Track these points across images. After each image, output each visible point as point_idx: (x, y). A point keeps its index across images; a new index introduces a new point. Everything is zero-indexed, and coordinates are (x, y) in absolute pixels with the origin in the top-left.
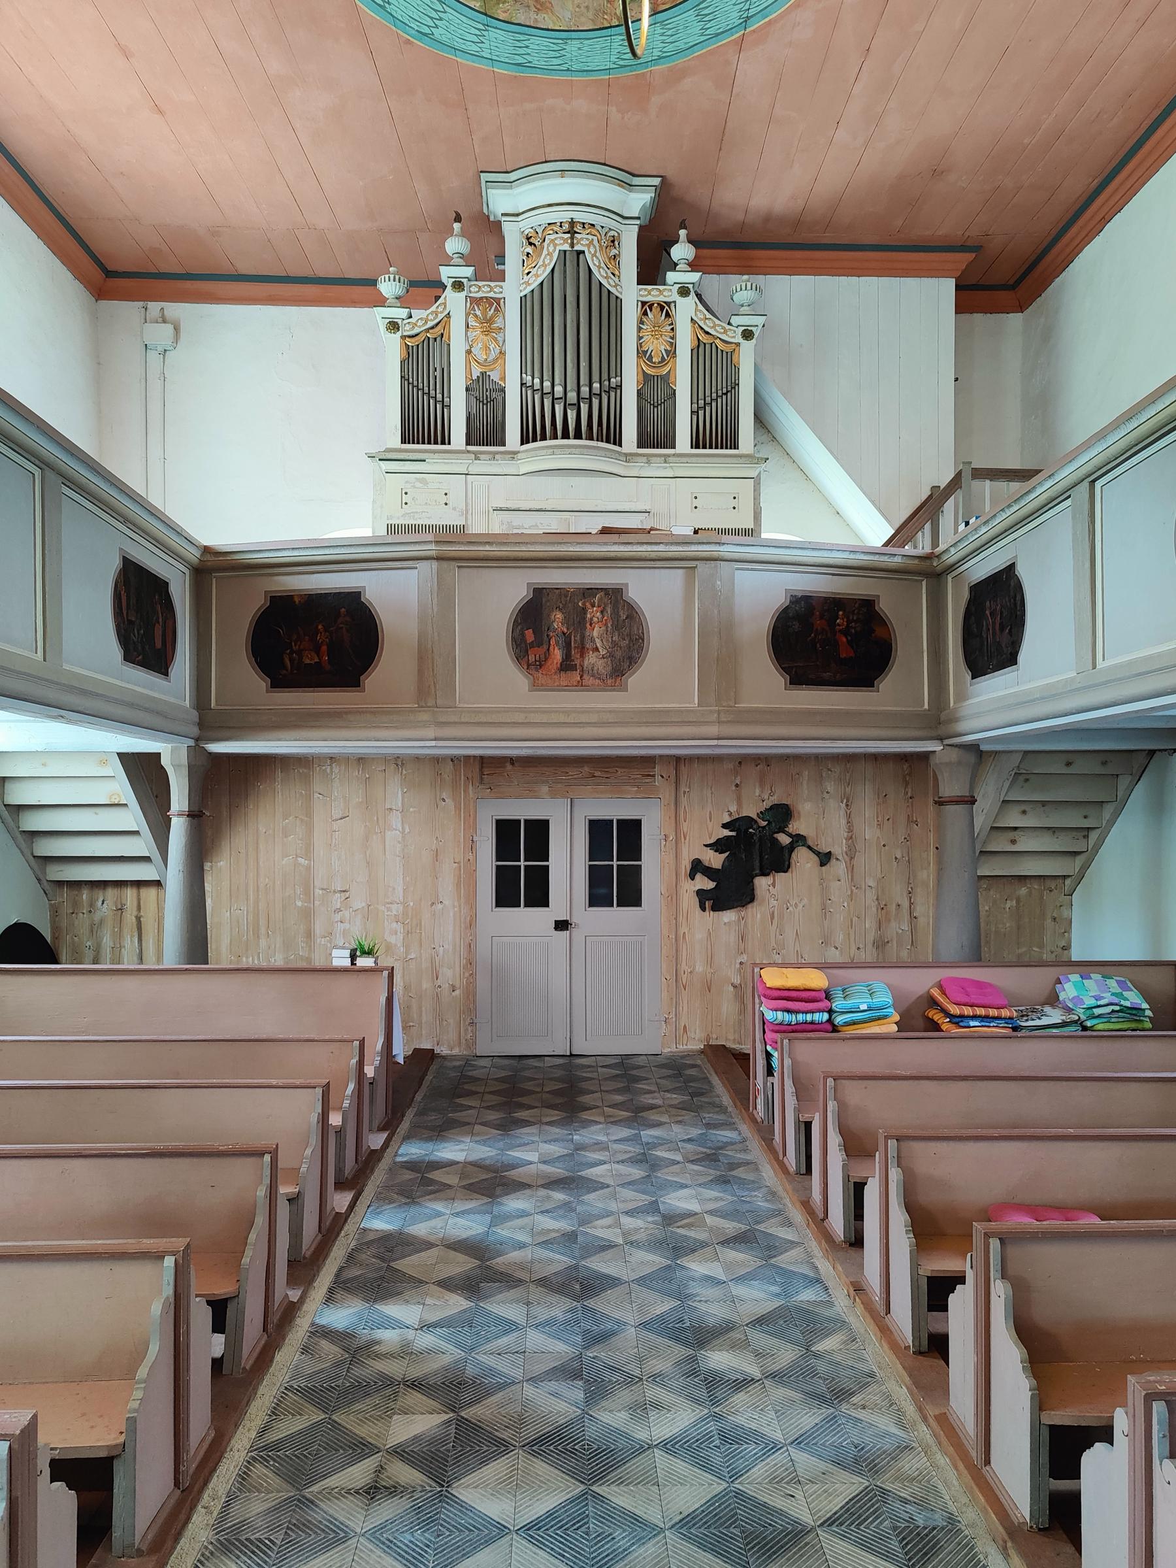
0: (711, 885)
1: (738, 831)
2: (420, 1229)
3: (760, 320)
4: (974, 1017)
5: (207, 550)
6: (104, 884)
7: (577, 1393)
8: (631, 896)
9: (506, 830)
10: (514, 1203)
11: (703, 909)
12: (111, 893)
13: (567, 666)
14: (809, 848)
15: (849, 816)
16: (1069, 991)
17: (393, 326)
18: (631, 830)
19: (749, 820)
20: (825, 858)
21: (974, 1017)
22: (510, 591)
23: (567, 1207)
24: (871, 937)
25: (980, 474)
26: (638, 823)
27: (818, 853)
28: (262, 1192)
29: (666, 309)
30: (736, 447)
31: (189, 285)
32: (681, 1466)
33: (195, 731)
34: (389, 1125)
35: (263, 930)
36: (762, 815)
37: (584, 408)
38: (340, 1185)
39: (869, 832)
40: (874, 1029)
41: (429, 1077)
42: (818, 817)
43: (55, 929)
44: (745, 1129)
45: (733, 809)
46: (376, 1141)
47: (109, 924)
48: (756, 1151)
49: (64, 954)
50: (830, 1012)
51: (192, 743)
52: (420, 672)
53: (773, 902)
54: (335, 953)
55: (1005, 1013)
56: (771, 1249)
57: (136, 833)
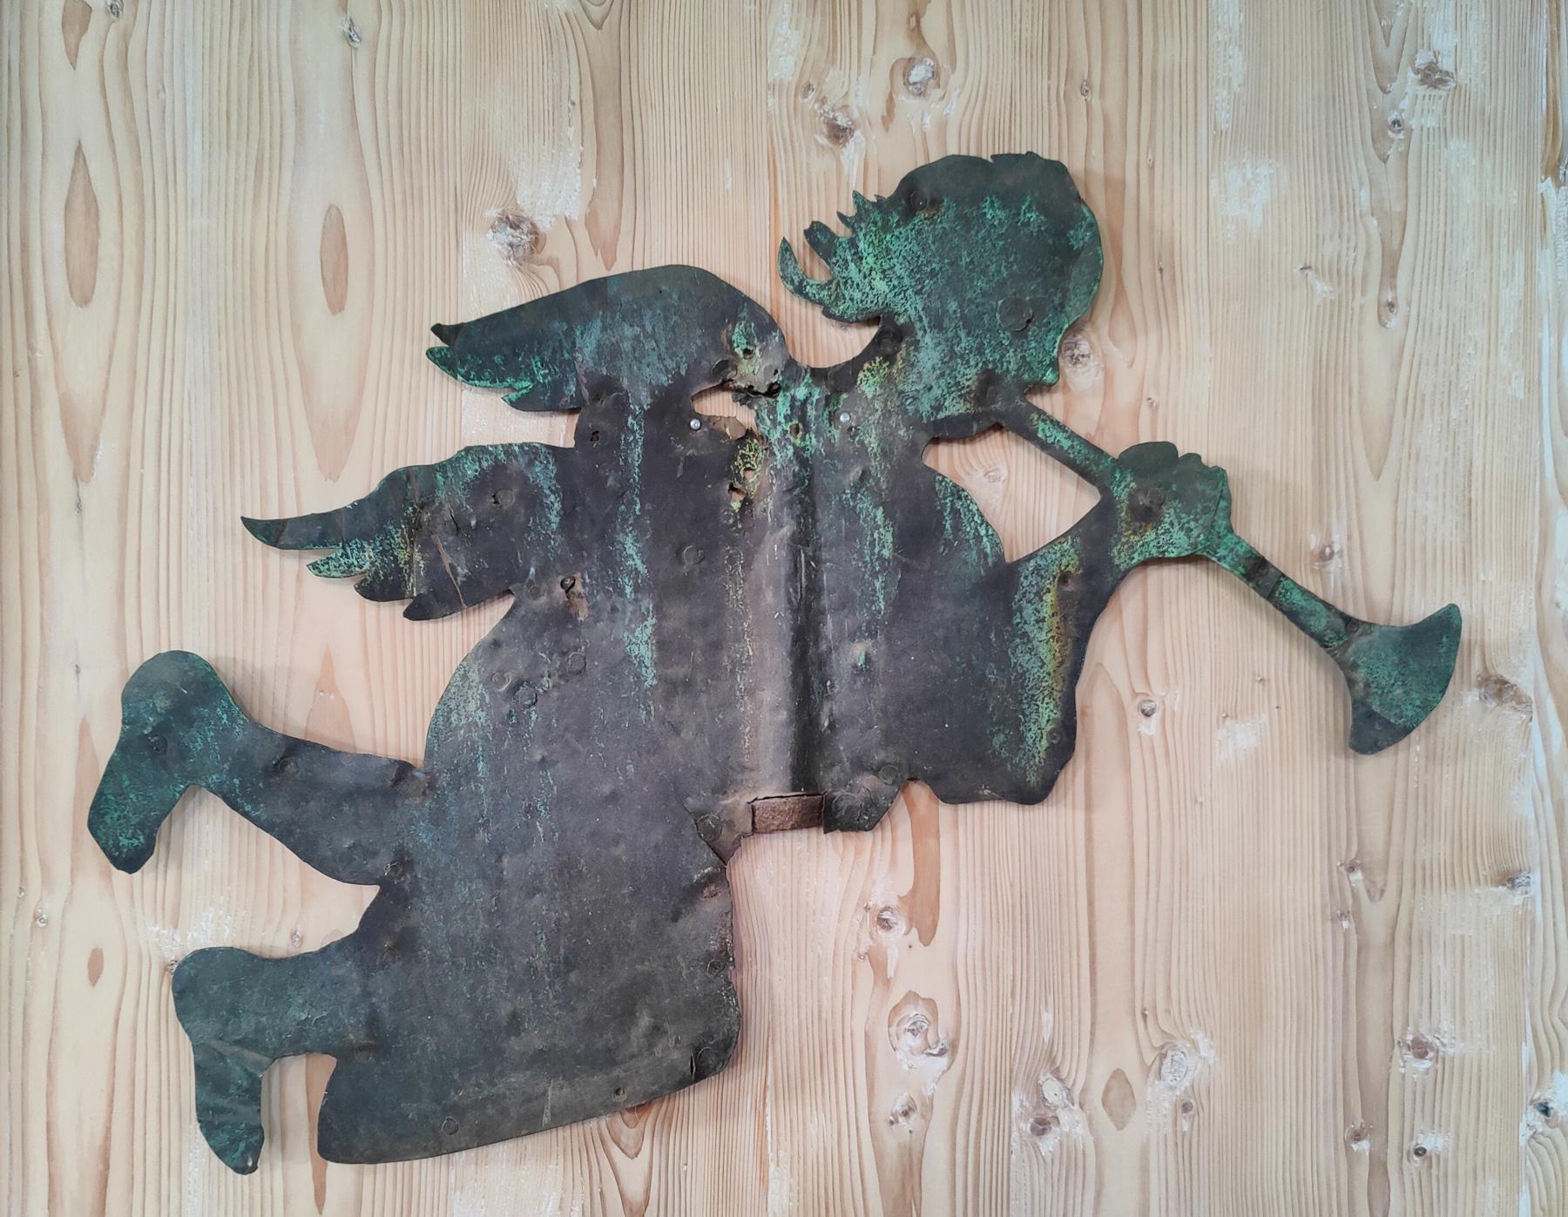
1: (597, 402)
11: (235, 1130)
14: (1257, 573)
20: (1393, 677)
27: (1332, 632)
45: (556, 192)
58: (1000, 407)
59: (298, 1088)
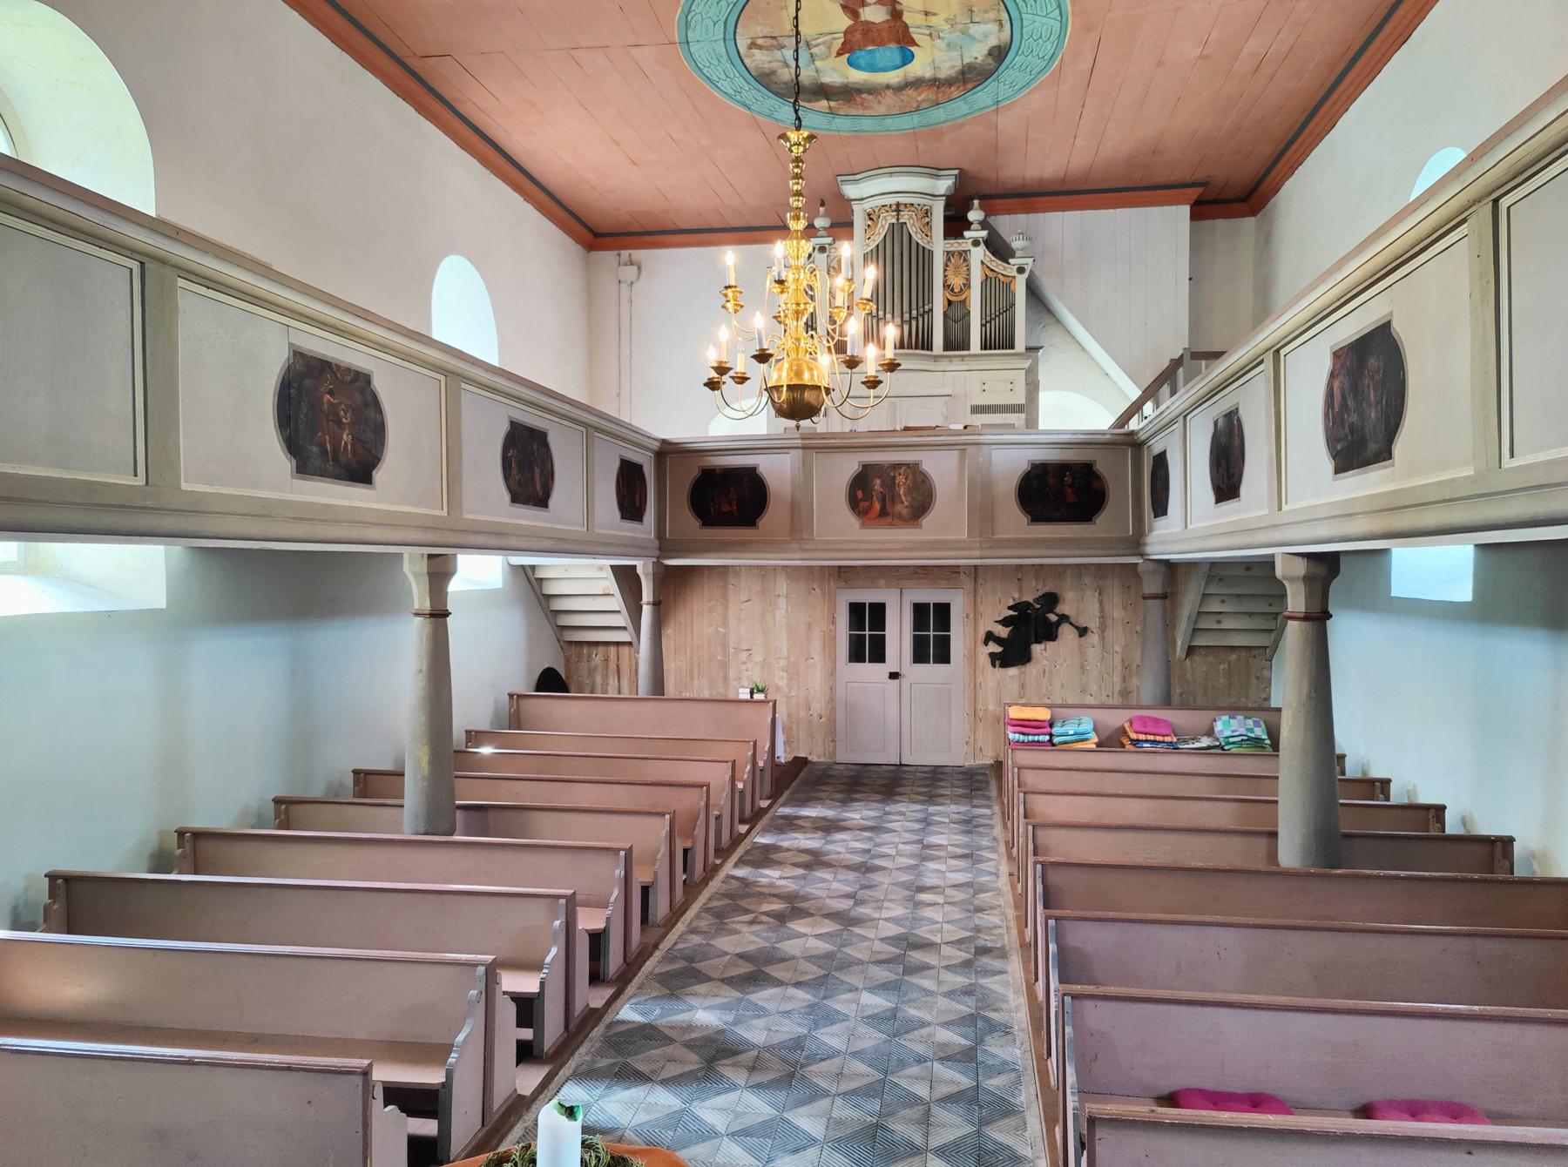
0: (999, 649)
2: (785, 844)
5: (664, 441)
6: (597, 644)
7: (851, 902)
8: (944, 657)
9: (856, 610)
10: (839, 836)
11: (994, 665)
12: (601, 649)
13: (883, 513)
15: (1101, 603)
16: (1219, 726)
18: (943, 611)
20: (1083, 632)
22: (849, 466)
23: (870, 839)
24: (1117, 688)
25: (1196, 356)
26: (948, 605)
29: (964, 255)
31: (647, 238)
33: (657, 553)
36: (1036, 600)
37: (906, 328)
38: (742, 821)
39: (1117, 613)
40: (1080, 746)
41: (802, 774)
42: (1077, 603)
44: (997, 809)
45: (1016, 595)
46: (765, 804)
48: (997, 821)
49: (572, 688)
50: (1051, 735)
52: (792, 518)
55: (1168, 739)
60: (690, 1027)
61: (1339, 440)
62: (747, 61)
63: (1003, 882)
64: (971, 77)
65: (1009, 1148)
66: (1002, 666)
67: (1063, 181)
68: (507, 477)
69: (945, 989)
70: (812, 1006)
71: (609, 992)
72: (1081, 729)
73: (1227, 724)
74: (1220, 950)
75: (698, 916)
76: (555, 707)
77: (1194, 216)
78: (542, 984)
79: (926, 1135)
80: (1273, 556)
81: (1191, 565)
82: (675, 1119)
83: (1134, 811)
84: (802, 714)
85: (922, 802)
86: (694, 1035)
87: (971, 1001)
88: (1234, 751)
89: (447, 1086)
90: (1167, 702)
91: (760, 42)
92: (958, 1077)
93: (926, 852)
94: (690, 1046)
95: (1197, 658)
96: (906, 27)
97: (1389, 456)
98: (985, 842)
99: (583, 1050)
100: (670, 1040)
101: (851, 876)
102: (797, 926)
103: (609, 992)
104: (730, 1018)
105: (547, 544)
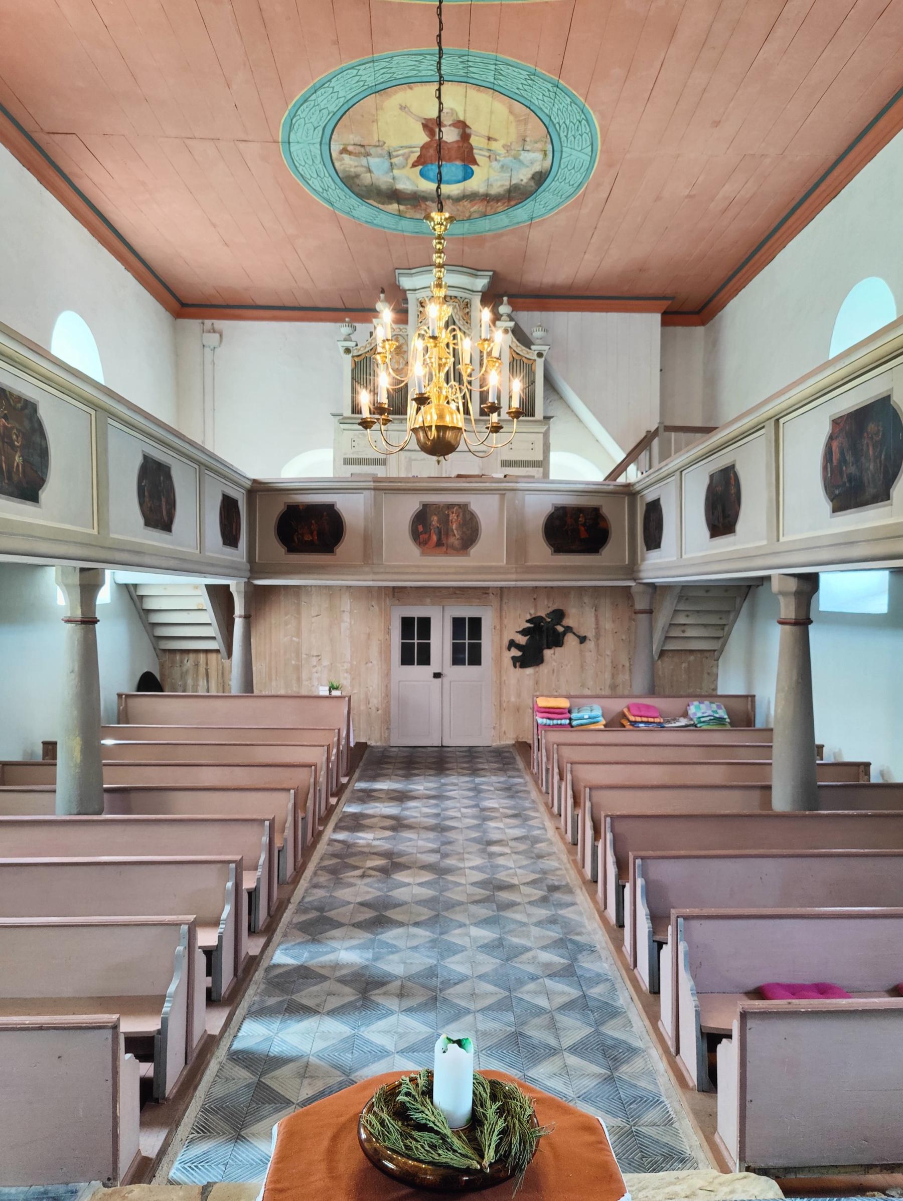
0: (519, 654)
2: (370, 812)
3: (547, 348)
4: (642, 722)
5: (255, 481)
7: (438, 856)
8: (475, 660)
9: (407, 624)
11: (515, 667)
12: (192, 656)
13: (439, 544)
15: (596, 617)
16: (692, 710)
17: (348, 351)
18: (476, 623)
19: (541, 618)
20: (583, 640)
21: (642, 722)
22: (411, 505)
23: (437, 805)
24: (608, 682)
25: (668, 429)
28: (312, 780)
30: (533, 415)
31: (228, 311)
32: (474, 872)
33: (248, 574)
34: (349, 773)
35: (274, 677)
36: (548, 615)
38: (333, 795)
39: (608, 625)
40: (592, 727)
41: (365, 756)
42: (579, 618)
43: (162, 674)
44: (528, 778)
45: (532, 612)
46: (344, 780)
47: (191, 672)
48: (531, 786)
49: (167, 687)
50: (570, 719)
51: (246, 580)
52: (365, 546)
53: (554, 664)
54: (321, 688)
55: (657, 720)
56: (527, 819)
57: (210, 624)
58: (559, 623)
59: (518, 664)
60: (336, 966)
61: (837, 487)
62: (337, 164)
63: (551, 834)
64: (515, 195)
65: (625, 1042)
66: (522, 666)
67: (570, 287)
68: (141, 504)
69: (534, 920)
70: (434, 941)
71: (262, 941)
72: (594, 714)
73: (698, 708)
74: (760, 877)
75: (315, 874)
76: (150, 703)
77: (664, 323)
78: (220, 938)
79: (557, 1037)
80: (768, 578)
81: (666, 588)
82: (350, 1043)
83: (655, 774)
84: (363, 708)
85: (469, 775)
86: (344, 972)
87: (557, 928)
88: (705, 727)
89: (162, 1032)
90: (653, 692)
91: (350, 148)
92: (567, 989)
93: (484, 816)
94: (342, 981)
95: (666, 659)
96: (471, 148)
97: (888, 497)
98: (527, 804)
99: (251, 991)
100: (324, 978)
101: (432, 835)
102: (401, 877)
103: (262, 941)
104: (369, 955)
105: (172, 563)
